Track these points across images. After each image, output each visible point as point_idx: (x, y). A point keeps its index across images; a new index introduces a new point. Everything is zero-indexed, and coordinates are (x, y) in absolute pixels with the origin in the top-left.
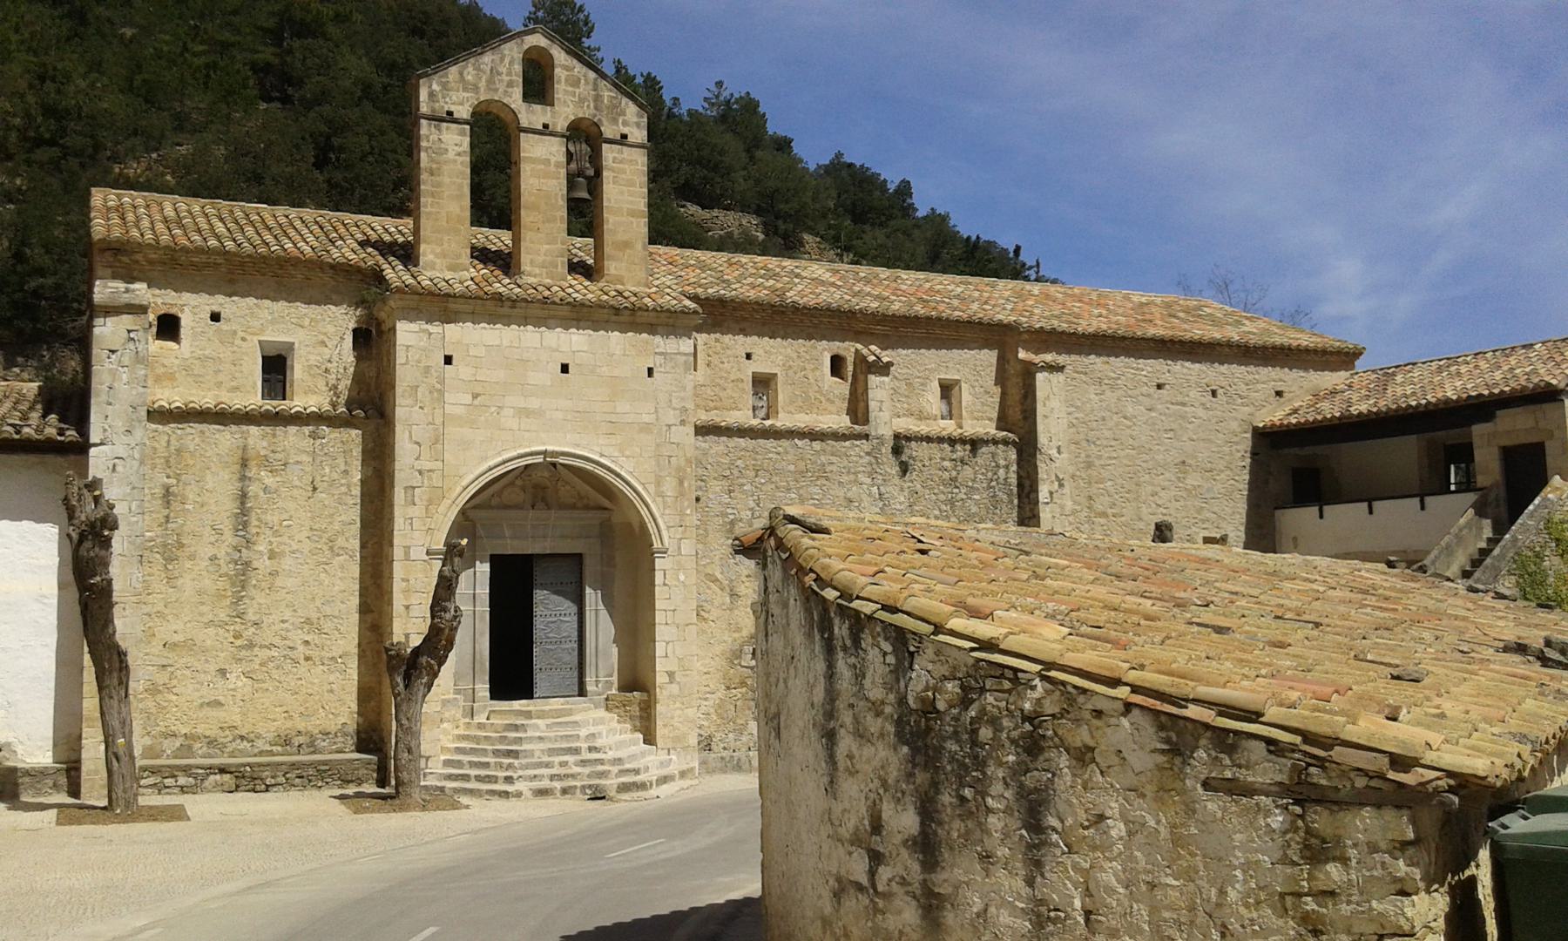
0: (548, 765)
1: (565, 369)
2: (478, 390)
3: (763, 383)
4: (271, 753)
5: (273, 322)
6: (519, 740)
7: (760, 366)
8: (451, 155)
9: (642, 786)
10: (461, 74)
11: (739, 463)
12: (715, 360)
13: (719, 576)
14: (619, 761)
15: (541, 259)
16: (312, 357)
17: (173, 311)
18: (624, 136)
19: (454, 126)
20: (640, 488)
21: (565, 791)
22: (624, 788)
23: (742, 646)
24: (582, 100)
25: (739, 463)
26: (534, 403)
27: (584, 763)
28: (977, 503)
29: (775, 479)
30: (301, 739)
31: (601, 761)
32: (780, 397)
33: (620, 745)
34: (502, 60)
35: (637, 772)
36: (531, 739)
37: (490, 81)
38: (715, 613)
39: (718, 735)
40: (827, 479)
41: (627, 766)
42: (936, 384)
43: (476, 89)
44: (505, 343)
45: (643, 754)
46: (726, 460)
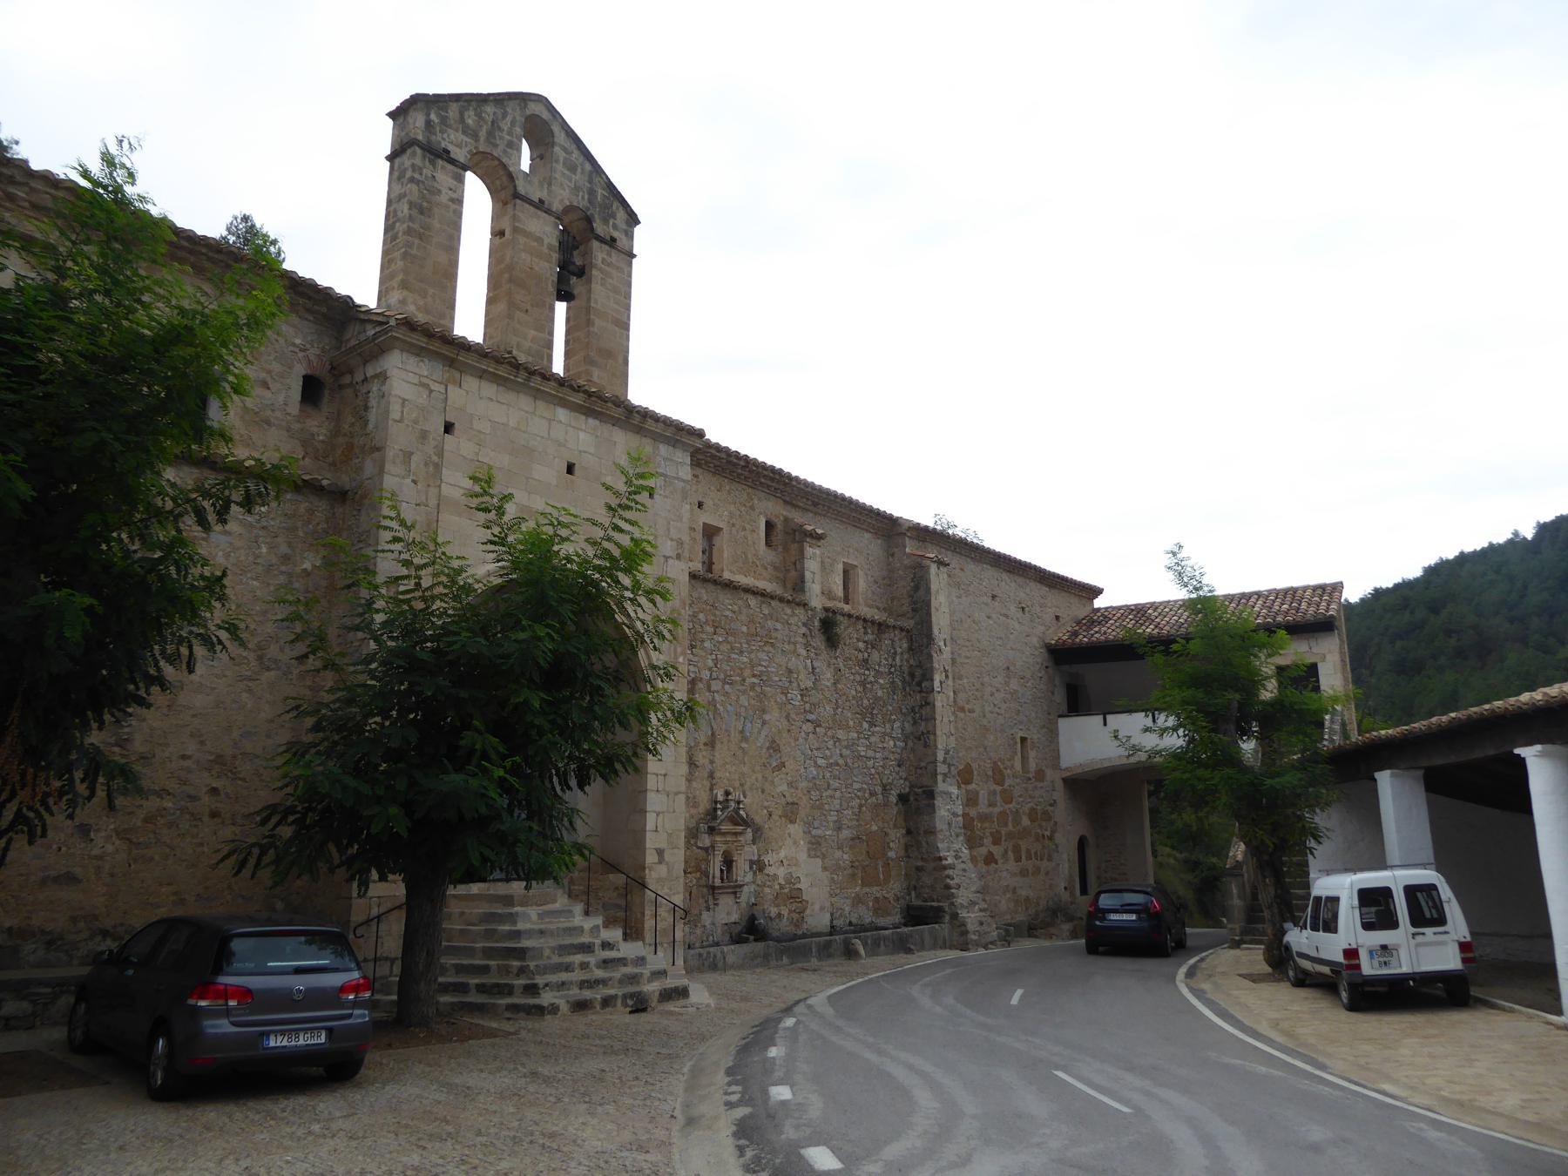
10: (462, 114)
11: (701, 616)
18: (613, 240)
19: (450, 167)
24: (577, 189)
25: (701, 616)
28: (882, 687)
37: (490, 134)
40: (772, 645)
42: (840, 567)
43: (475, 137)
44: (512, 423)
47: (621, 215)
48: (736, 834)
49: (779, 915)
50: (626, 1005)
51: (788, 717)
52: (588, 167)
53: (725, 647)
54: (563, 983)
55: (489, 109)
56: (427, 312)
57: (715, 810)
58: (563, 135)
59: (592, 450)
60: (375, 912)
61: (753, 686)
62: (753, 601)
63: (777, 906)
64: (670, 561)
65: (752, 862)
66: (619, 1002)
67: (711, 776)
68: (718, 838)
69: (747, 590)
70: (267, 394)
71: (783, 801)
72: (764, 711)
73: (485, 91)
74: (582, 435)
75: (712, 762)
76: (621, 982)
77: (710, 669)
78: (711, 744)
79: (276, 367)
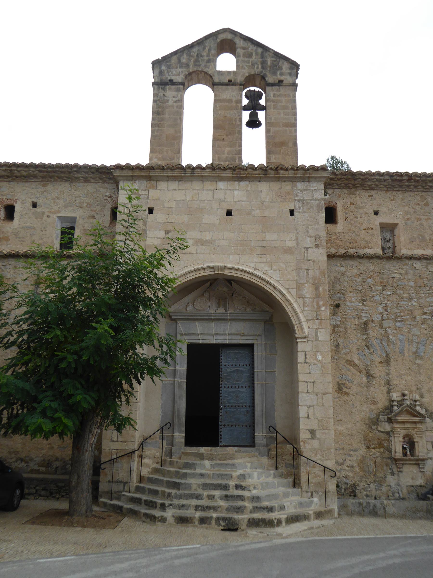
0: (198, 497)
1: (229, 213)
2: (169, 228)
3: (389, 228)
4: (38, 472)
5: (66, 206)
6: (185, 475)
7: (385, 218)
8: (171, 103)
9: (270, 523)
11: (369, 281)
12: (351, 216)
13: (357, 362)
14: (257, 499)
15: (224, 156)
16: (86, 225)
17: (12, 203)
18: (281, 81)
19: (173, 87)
20: (285, 292)
21: (202, 521)
22: (254, 523)
23: (378, 415)
24: (253, 65)
25: (369, 281)
26: (207, 236)
27: (227, 497)
29: (398, 292)
30: (58, 464)
31: (241, 498)
32: (402, 239)
33: (264, 486)
34: (204, 49)
35: (270, 509)
36: (194, 475)
37: (196, 61)
38: (354, 390)
39: (362, 485)
41: (265, 504)
43: (187, 66)
44: (188, 198)
45: (286, 495)
46: (359, 279)
47: (285, 66)
48: (415, 423)
50: (220, 525)
52: (260, 50)
53: (394, 298)
54: (183, 506)
55: (195, 50)
56: (164, 159)
57: (392, 406)
58: (242, 41)
59: (244, 199)
60: (114, 456)
61: (424, 322)
62: (418, 265)
64: (310, 250)
66: (213, 522)
67: (388, 383)
68: (396, 425)
69: (410, 258)
70: (94, 221)
73: (190, 42)
74: (236, 193)
75: (388, 374)
76: (228, 510)
77: (381, 313)
78: (387, 361)
79: (98, 208)
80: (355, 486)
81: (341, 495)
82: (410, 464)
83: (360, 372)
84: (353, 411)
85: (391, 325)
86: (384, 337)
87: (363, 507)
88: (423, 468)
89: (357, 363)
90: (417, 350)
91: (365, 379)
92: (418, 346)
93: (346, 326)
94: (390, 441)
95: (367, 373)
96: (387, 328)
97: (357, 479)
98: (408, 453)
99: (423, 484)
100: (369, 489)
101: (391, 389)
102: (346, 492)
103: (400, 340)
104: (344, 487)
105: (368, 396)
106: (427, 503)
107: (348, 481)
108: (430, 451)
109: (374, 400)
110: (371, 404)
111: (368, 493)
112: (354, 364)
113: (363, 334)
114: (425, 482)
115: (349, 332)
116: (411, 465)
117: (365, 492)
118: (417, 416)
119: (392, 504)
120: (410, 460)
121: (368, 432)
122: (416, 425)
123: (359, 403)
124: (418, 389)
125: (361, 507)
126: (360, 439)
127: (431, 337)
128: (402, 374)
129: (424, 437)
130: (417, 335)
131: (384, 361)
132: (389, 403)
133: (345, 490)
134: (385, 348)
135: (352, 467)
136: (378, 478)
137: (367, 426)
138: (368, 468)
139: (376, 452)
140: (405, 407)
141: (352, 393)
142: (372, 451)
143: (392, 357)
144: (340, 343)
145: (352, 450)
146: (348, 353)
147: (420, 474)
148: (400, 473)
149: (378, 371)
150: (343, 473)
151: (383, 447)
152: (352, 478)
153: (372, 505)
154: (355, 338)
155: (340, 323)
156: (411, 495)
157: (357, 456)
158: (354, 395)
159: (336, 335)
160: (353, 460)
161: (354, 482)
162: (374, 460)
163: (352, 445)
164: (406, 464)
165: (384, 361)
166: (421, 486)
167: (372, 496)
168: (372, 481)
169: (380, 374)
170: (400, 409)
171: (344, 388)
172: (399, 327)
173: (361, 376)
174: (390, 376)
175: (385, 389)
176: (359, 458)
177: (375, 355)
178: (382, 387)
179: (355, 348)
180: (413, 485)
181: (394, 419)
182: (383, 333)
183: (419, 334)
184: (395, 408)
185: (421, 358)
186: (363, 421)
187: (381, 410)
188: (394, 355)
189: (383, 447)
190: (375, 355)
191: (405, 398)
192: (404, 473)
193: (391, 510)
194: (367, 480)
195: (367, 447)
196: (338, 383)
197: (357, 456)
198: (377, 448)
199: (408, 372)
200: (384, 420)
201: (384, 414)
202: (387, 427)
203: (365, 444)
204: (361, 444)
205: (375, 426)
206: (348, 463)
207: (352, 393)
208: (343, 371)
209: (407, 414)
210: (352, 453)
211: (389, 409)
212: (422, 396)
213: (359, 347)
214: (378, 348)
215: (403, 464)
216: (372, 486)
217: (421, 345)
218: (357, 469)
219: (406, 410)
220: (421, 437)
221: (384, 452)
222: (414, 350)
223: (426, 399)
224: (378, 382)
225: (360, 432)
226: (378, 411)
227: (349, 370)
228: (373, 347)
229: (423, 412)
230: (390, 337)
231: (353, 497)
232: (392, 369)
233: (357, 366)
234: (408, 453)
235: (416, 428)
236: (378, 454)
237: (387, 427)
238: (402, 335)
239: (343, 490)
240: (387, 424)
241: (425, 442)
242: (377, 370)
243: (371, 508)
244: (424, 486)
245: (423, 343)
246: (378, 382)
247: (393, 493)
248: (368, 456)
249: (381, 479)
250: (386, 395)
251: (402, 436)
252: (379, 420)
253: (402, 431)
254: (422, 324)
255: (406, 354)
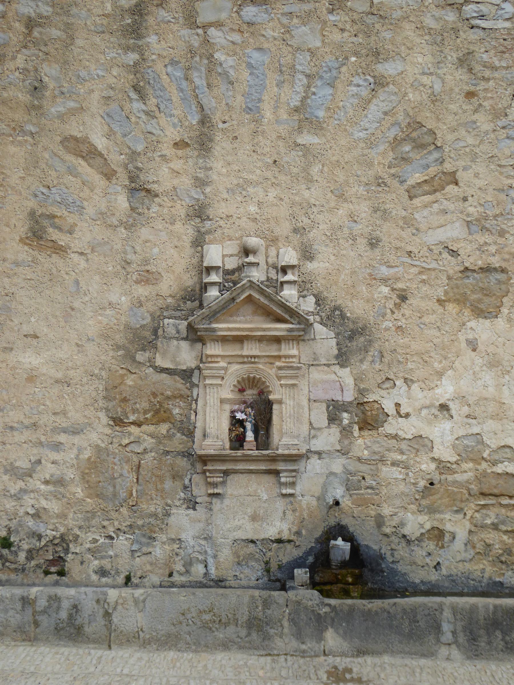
13: (100, 142)
23: (157, 319)
38: (86, 233)
39: (87, 538)
48: (277, 340)
49: (438, 534)
51: (465, 61)
57: (205, 287)
63: (432, 510)
65: (335, 411)
67: (199, 212)
71: (452, 266)
72: (376, 54)
75: (201, 183)
78: (201, 140)
80: (63, 541)
81: (16, 570)
82: (251, 472)
83: (109, 175)
84: (77, 304)
85: (224, 16)
86: (197, 59)
87: (34, 613)
88: (293, 484)
89: (100, 147)
90: (305, 98)
91: (122, 202)
92: (309, 87)
93: (71, 20)
94: (190, 401)
95: (132, 179)
96: (211, 25)
97: (73, 521)
98: (250, 436)
99: (285, 536)
100: (111, 553)
101: (209, 232)
102: (33, 563)
103: (250, 66)
104: (26, 547)
105: (130, 257)
106: (253, 597)
107: (42, 529)
108: (319, 429)
109: (148, 268)
110: (137, 282)
111: (107, 564)
112: (90, 152)
113: (127, 49)
114: (295, 529)
115: (79, 42)
116: (253, 476)
117: (96, 562)
118: (279, 320)
119: (136, 601)
120: (247, 459)
121: (121, 372)
122: (280, 350)
123: (97, 278)
124: (296, 231)
125: (29, 611)
126: (94, 394)
127: (356, 54)
128: (250, 183)
129: (303, 384)
130: (309, 50)
131: (191, 138)
132: (196, 279)
133: (30, 556)
134: (197, 96)
135: (60, 482)
136: (142, 517)
137: (120, 353)
138: (114, 487)
139: (144, 437)
140: (243, 289)
141: (77, 245)
142: (130, 434)
143: (221, 125)
144: (46, 79)
145: (65, 431)
146: (73, 112)
147: (280, 504)
148: (214, 500)
149: (170, 174)
150: (29, 500)
151: (168, 419)
152: (58, 516)
153: (66, 604)
154: (97, 61)
155: (50, 9)
156: (247, 571)
157: (80, 450)
158: (82, 254)
159: (33, 51)
160: (65, 462)
161: (62, 529)
162: (135, 459)
163: (64, 413)
164: (236, 472)
165: (191, 138)
166: (279, 541)
167: (118, 573)
168: (123, 528)
169: (176, 182)
170: (227, 295)
171: (51, 230)
172: (250, 24)
173: (110, 190)
174: (208, 190)
175: (186, 232)
176: (86, 454)
177: (163, 120)
178: (178, 227)
179: (96, 96)
180: (255, 538)
181: (206, 330)
182: (196, 44)
183: (319, 44)
184: (213, 293)
185: (317, 126)
186: (106, 337)
187: (169, 300)
188: (227, 118)
189: (168, 419)
190: (163, 120)
191: (251, 259)
192: (227, 502)
193: (128, 619)
194: (106, 523)
195: (114, 419)
196: (32, 214)
197: (80, 450)
198: (146, 422)
199: (269, 174)
200: (178, 332)
201: (178, 314)
202: (186, 356)
203: (107, 410)
204: (96, 410)
205: (147, 354)
206: (48, 470)
207: (77, 245)
208: (53, 173)
209: (255, 313)
210: (62, 438)
211: (196, 295)
212: (307, 254)
213: (112, 93)
214: (175, 96)
215: (226, 473)
216: (122, 542)
217: (319, 83)
218: (79, 491)
219: (250, 299)
220: (294, 385)
221: (169, 437)
222: (295, 102)
223: (322, 265)
224: (166, 211)
225: (96, 372)
226: (161, 303)
227: (72, 171)
228: (159, 93)
229: (308, 305)
230: (219, 56)
231: (55, 577)
232: (218, 165)
233: (101, 155)
234: (250, 436)
235: (279, 357)
236: (149, 442)
237: (186, 356)
238: (260, 49)
239: (22, 556)
240: (184, 345)
241: (305, 403)
242: (165, 170)
243: (64, 615)
244: (289, 541)
245: (327, 76)
246: (166, 211)
247: (188, 564)
248: (114, 448)
249: (152, 520)
250: (189, 251)
251: (231, 381)
252: (160, 332)
253: (235, 368)
254: (331, 12)
255: (268, 114)
